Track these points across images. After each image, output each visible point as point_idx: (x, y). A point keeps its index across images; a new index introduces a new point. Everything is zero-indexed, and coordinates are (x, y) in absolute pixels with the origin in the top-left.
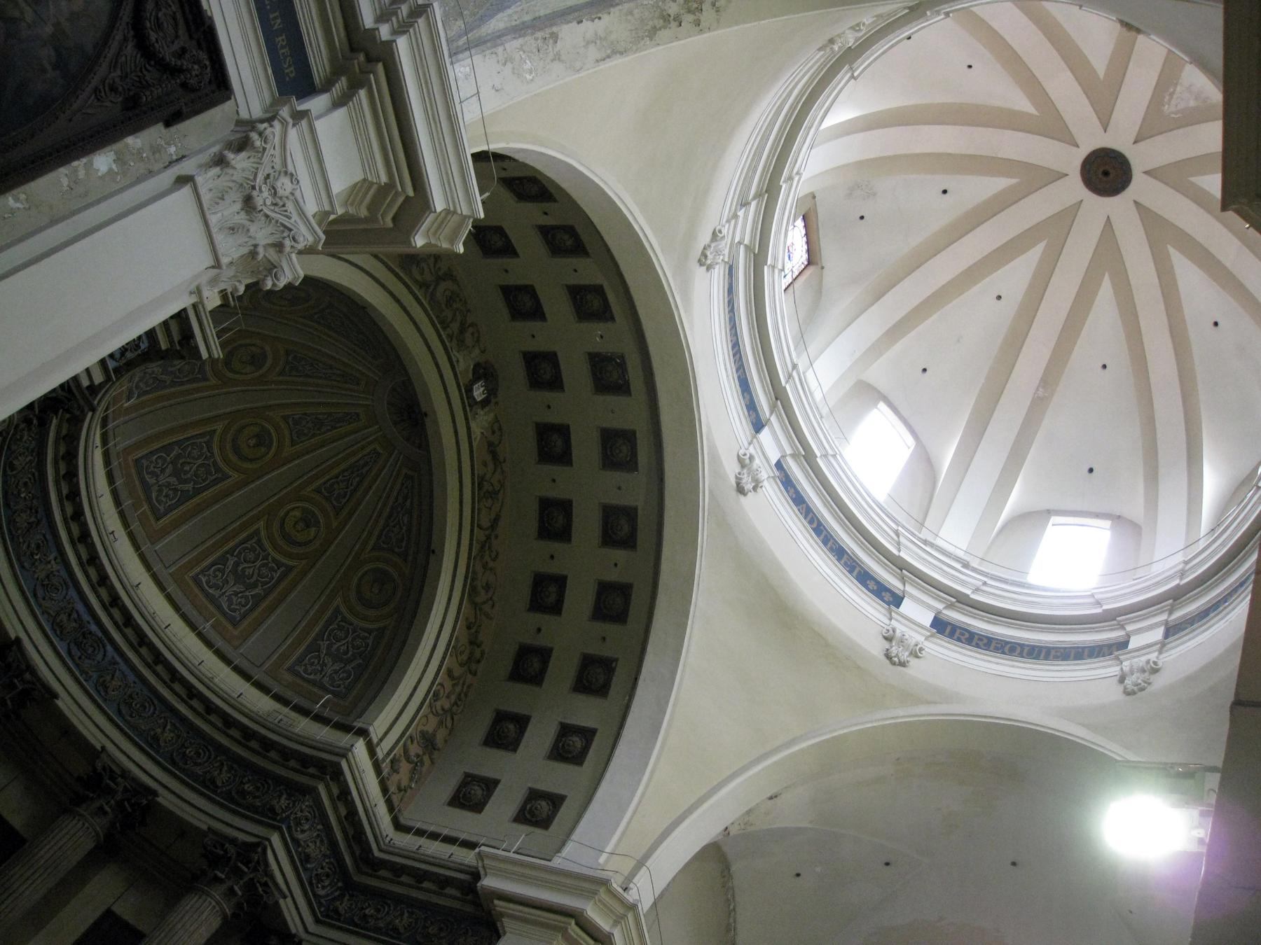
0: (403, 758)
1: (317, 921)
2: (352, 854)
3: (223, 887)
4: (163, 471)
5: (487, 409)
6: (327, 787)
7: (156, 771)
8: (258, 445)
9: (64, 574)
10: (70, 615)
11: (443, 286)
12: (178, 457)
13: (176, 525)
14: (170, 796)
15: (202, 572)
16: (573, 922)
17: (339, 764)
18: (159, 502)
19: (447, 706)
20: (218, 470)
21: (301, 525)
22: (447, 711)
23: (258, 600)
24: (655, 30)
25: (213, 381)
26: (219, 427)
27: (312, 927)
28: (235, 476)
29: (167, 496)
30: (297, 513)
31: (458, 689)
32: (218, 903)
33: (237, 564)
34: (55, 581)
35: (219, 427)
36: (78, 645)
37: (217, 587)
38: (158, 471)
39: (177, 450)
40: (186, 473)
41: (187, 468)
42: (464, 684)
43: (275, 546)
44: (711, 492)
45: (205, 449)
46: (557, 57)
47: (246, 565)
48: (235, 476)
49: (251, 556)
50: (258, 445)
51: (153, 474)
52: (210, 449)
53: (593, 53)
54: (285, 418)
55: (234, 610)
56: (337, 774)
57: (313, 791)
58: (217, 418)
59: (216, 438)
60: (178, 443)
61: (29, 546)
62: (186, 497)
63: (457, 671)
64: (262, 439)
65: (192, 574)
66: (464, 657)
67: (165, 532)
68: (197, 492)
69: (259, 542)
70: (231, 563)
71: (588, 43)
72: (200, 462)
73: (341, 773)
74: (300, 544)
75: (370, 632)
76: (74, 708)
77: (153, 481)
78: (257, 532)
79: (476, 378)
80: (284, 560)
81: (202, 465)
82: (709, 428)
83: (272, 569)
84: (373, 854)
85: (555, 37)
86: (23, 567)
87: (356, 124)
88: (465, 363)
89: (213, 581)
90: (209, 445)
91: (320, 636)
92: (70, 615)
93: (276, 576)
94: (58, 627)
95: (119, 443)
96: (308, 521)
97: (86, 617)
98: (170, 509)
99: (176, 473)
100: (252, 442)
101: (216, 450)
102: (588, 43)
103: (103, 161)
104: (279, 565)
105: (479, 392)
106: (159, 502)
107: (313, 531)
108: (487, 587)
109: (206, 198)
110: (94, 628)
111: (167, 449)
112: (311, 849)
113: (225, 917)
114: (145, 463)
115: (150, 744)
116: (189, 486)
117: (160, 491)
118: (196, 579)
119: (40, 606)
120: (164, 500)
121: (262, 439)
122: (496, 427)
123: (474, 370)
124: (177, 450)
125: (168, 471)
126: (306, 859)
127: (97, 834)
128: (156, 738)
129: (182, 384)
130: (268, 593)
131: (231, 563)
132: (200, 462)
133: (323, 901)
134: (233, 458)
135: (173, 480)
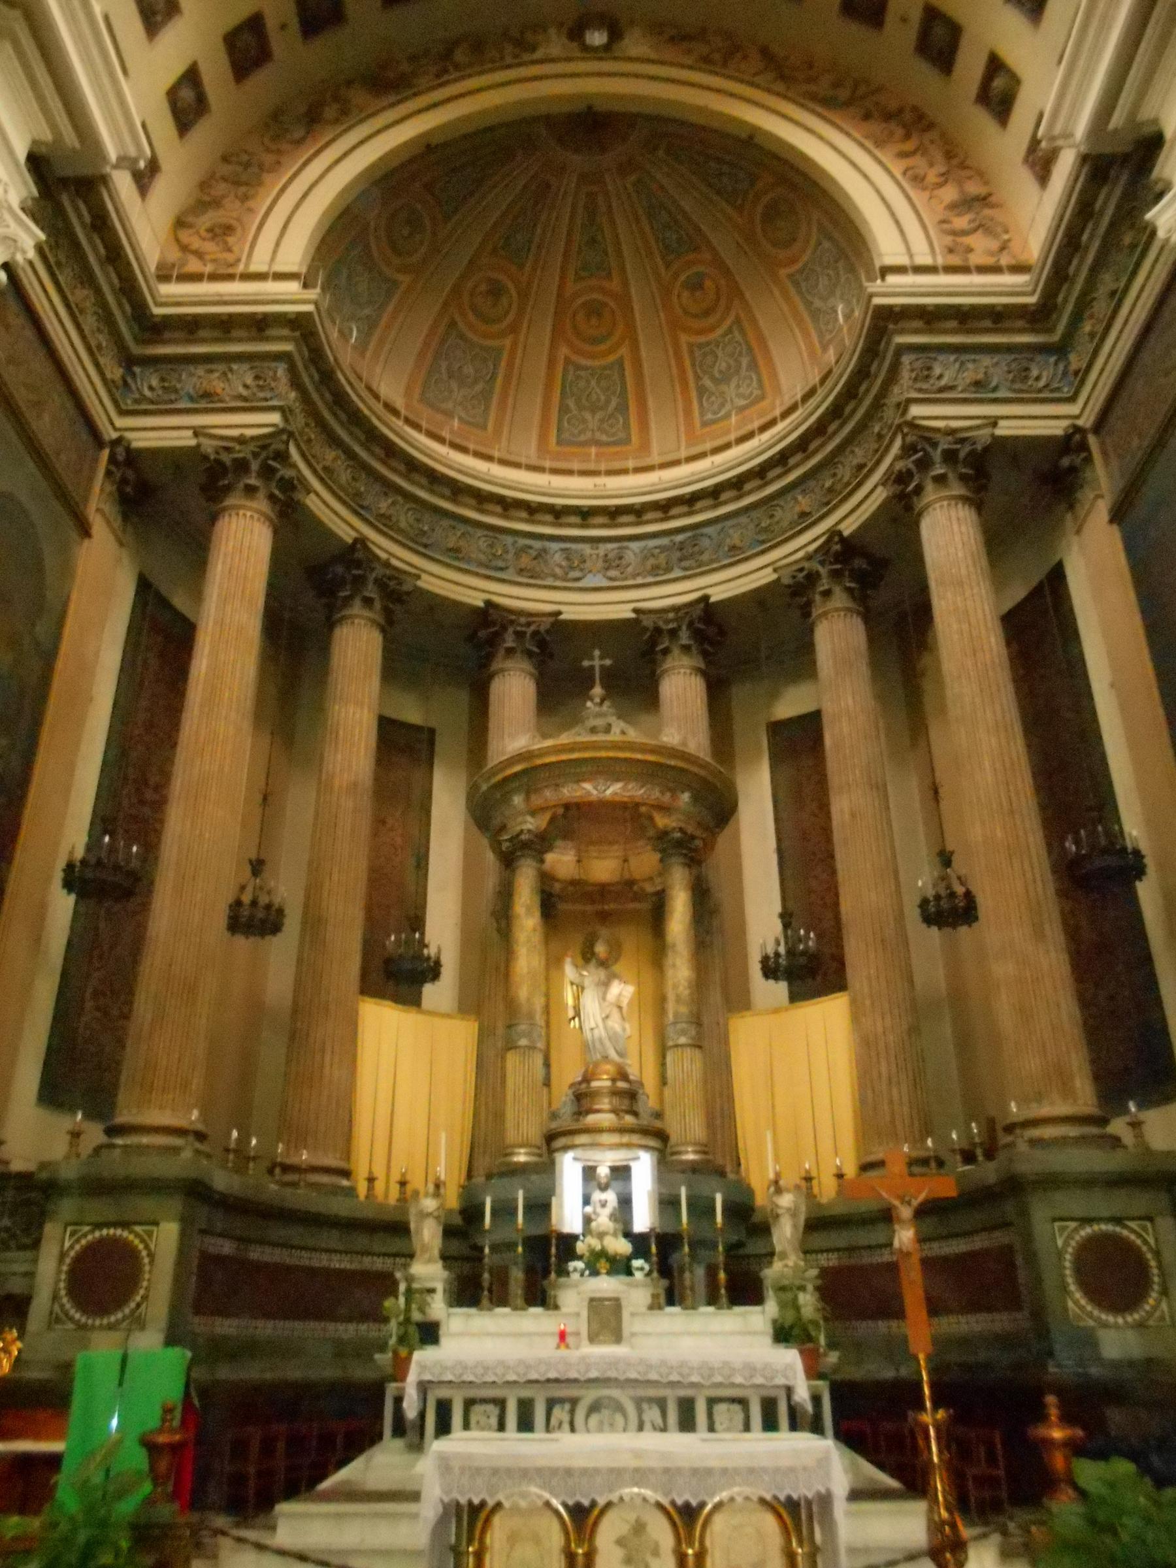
1: (1072, 399)
2: (1021, 331)
3: (929, 487)
8: (599, 315)
9: (610, 546)
10: (653, 555)
12: (578, 402)
15: (702, 414)
18: (614, 435)
19: (943, 169)
20: (610, 367)
21: (698, 294)
22: (948, 172)
27: (1074, 409)
28: (624, 351)
29: (612, 426)
32: (941, 499)
34: (611, 556)
37: (723, 405)
38: (581, 427)
39: (571, 403)
40: (599, 400)
41: (594, 397)
45: (582, 373)
47: (716, 368)
48: (624, 351)
49: (709, 359)
50: (599, 315)
52: (586, 368)
55: (751, 393)
59: (575, 358)
61: (561, 567)
62: (623, 408)
63: (909, 146)
65: (697, 422)
69: (700, 346)
72: (593, 383)
73: (890, 308)
74: (718, 299)
75: (819, 243)
76: (732, 584)
77: (589, 435)
81: (598, 382)
84: (1032, 305)
86: (501, 569)
88: (556, 44)
89: (715, 407)
91: (809, 304)
92: (653, 555)
94: (655, 570)
95: (530, 453)
96: (695, 285)
97: (665, 541)
98: (626, 426)
100: (594, 321)
104: (730, 331)
105: (597, 38)
106: (614, 435)
107: (708, 283)
108: (836, 85)
110: (680, 538)
111: (564, 409)
112: (971, 373)
113: (965, 499)
115: (805, 520)
116: (614, 402)
118: (705, 424)
119: (626, 579)
120: (614, 430)
121: (594, 310)
124: (571, 403)
126: (978, 384)
127: (848, 609)
128: (804, 515)
130: (750, 350)
132: (593, 383)
133: (1056, 385)
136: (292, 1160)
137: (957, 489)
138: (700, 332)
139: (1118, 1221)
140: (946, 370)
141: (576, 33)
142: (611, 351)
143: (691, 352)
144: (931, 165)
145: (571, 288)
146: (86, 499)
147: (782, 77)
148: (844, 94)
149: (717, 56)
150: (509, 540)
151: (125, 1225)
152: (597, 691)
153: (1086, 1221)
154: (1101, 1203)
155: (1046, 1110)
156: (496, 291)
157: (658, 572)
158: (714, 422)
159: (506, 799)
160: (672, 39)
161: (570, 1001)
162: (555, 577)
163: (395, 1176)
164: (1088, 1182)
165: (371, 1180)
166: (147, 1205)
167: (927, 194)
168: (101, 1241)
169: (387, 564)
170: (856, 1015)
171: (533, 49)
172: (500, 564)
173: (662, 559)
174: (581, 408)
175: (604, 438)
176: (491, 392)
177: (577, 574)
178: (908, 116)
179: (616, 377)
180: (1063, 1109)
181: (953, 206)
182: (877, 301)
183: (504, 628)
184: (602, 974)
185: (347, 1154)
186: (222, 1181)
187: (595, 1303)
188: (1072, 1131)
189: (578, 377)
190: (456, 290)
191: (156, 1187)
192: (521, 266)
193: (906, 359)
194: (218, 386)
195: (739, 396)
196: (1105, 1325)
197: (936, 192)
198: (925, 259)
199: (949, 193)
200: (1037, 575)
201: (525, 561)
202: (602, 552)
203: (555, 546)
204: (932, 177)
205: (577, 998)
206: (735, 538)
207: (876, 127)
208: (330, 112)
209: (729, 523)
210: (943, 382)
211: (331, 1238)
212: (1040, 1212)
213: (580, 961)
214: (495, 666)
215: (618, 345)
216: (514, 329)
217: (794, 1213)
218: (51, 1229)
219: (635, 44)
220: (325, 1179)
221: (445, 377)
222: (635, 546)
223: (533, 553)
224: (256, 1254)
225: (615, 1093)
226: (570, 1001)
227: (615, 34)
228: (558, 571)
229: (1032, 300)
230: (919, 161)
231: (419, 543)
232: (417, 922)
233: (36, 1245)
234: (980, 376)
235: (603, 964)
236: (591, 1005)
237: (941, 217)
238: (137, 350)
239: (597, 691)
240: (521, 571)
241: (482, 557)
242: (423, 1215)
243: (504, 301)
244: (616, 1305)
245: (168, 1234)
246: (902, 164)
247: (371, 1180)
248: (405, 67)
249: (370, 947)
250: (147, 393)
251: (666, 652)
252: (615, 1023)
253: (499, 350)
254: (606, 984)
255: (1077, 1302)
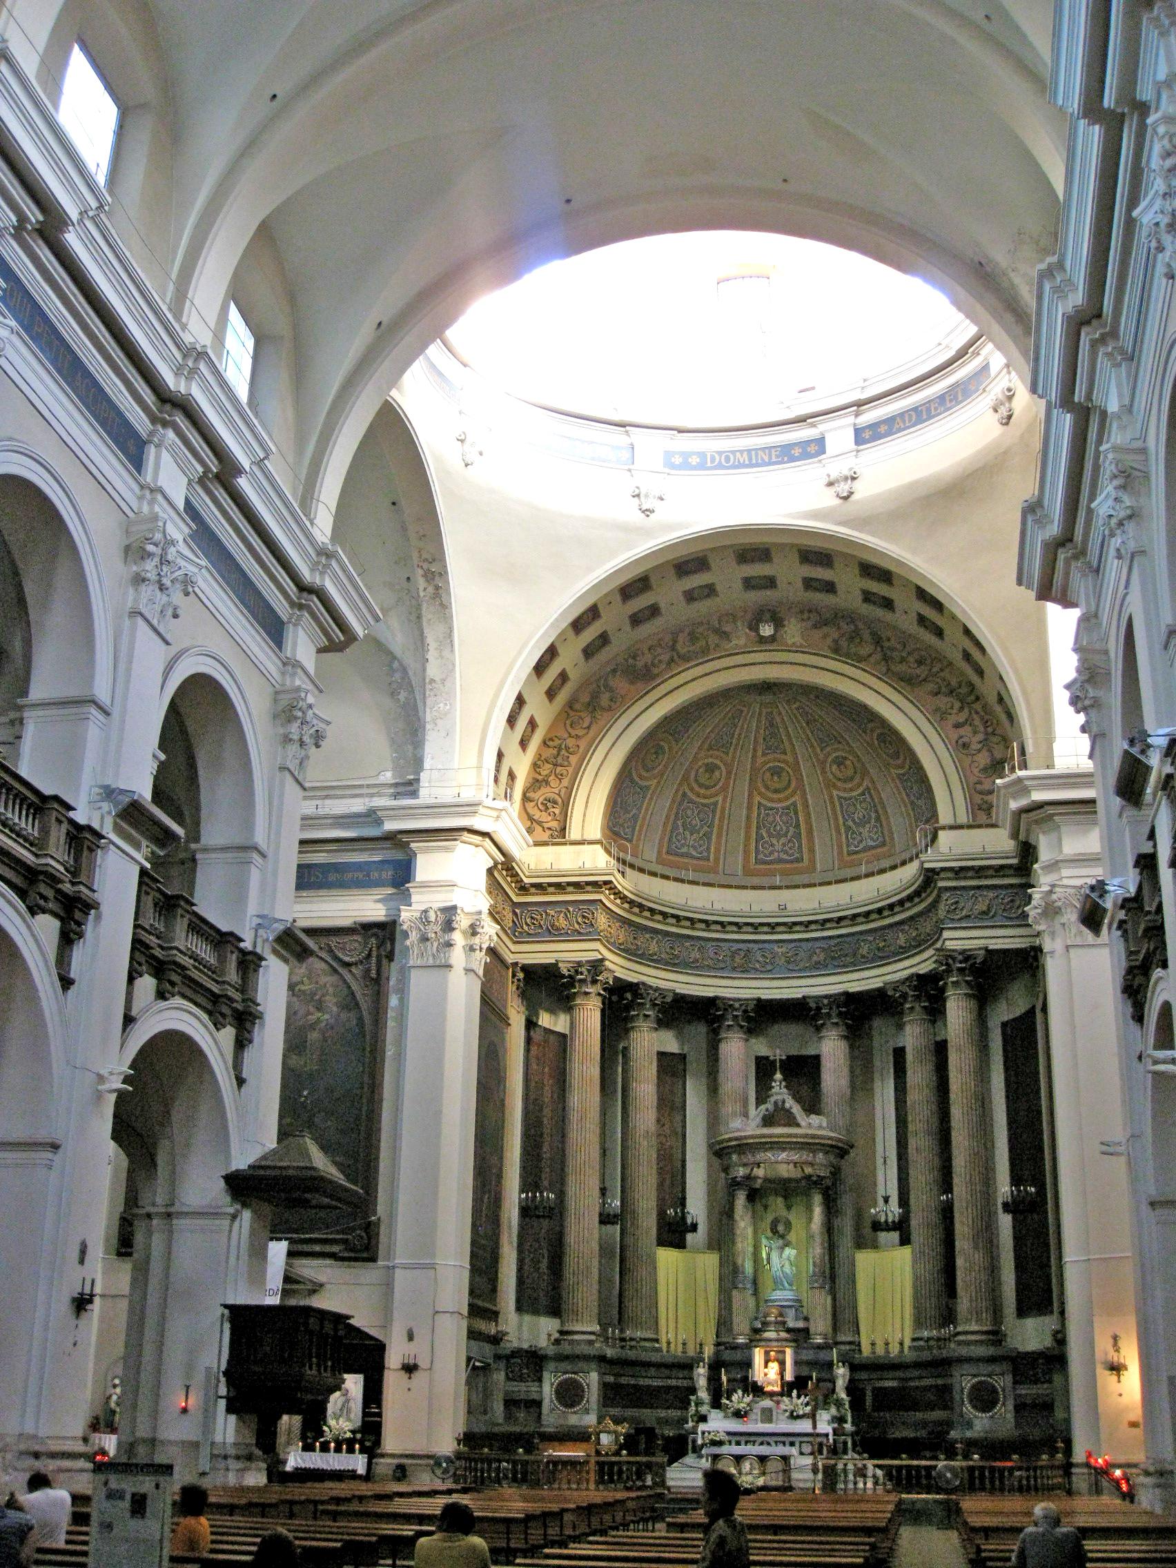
0: (986, 798)
4: (772, 845)
5: (786, 623)
6: (943, 879)
7: (907, 963)
8: (779, 777)
11: (679, 647)
12: (768, 832)
13: (812, 850)
14: (923, 965)
15: (848, 846)
16: (1024, 816)
17: (928, 870)
19: (981, 737)
20: (788, 808)
23: (878, 819)
24: (442, 604)
25: (720, 799)
26: (757, 799)
28: (796, 798)
30: (834, 767)
31: (977, 722)
33: (853, 821)
35: (757, 799)
36: (833, 958)
42: (977, 713)
43: (851, 790)
44: (840, 524)
46: (443, 681)
49: (852, 809)
50: (779, 777)
51: (771, 853)
53: (446, 653)
54: (764, 754)
56: (932, 870)
57: (940, 888)
58: (750, 796)
60: (758, 828)
62: (798, 835)
64: (777, 772)
66: (957, 705)
67: (812, 861)
68: (798, 826)
70: (850, 823)
71: (442, 657)
72: (778, 818)
78: (840, 798)
79: (757, 630)
80: (861, 789)
82: (790, 515)
83: (865, 800)
85: (432, 681)
87: (427, 850)
88: (742, 636)
90: (767, 808)
93: (869, 800)
94: (817, 966)
96: (840, 762)
99: (779, 836)
101: (774, 805)
102: (442, 657)
103: (393, 1001)
104: (863, 794)
105: (767, 630)
107: (848, 762)
108: (920, 662)
109: (419, 963)
110: (833, 942)
111: (759, 838)
114: (761, 856)
117: (786, 853)
118: (849, 854)
121: (777, 772)
122: (806, 616)
123: (750, 629)
125: (774, 841)
129: (713, 821)
131: (850, 823)
132: (778, 818)
134: (781, 796)
135: (783, 840)
136: (633, 1336)
137: (965, 990)
138: (845, 790)
139: (989, 1376)
140: (967, 906)
141: (754, 627)
142: (787, 798)
143: (841, 805)
144: (975, 733)
145: (760, 760)
146: (505, 1007)
147: (886, 659)
148: (922, 671)
149: (844, 643)
150: (727, 944)
151: (575, 1373)
152: (778, 1076)
153: (975, 1376)
154: (985, 1368)
155: (967, 1328)
156: (711, 769)
157: (817, 968)
158: (856, 853)
159: (730, 1153)
160: (815, 626)
161: (764, 1255)
162: (756, 970)
163: (680, 1341)
164: (979, 1360)
165: (669, 1343)
166: (581, 1365)
167: (968, 761)
168: (566, 1380)
169: (657, 989)
170: (914, 1261)
171: (725, 636)
172: (722, 965)
173: (822, 956)
174: (770, 835)
175: (785, 857)
176: (711, 832)
177: (769, 968)
178: (964, 690)
179: (792, 814)
180: (976, 1328)
181: (985, 770)
182: (927, 865)
183: (726, 1010)
184: (781, 1242)
185: (657, 1331)
186: (609, 1352)
187: (764, 1410)
188: (983, 1337)
189: (768, 815)
190: (685, 778)
191: (587, 1358)
192: (727, 754)
193: (945, 896)
194: (562, 922)
195: (872, 839)
196: (976, 1417)
197: (975, 758)
198: (963, 818)
199: (983, 759)
200: (1028, 1007)
201: (737, 959)
202: (784, 950)
203: (756, 946)
204: (975, 746)
205: (768, 1255)
206: (864, 950)
207: (943, 701)
208: (604, 700)
209: (862, 937)
210: (964, 913)
211: (652, 1371)
212: (956, 1374)
213: (770, 1234)
214: (723, 1035)
215: (794, 793)
216: (724, 789)
217: (844, 1376)
218: (546, 1375)
219: (793, 631)
220: (647, 1344)
221: (681, 830)
222: (804, 944)
223: (742, 954)
224: (624, 1380)
225: (776, 1323)
226: (764, 1255)
227: (778, 623)
228: (758, 966)
229: (1015, 861)
230: (966, 731)
231: (673, 964)
232: (683, 1202)
233: (540, 1380)
234: (985, 908)
235: (782, 1237)
236: (775, 1256)
237: (976, 780)
238: (516, 899)
239: (778, 1076)
240: (734, 969)
241: (710, 962)
242: (699, 1375)
243: (717, 773)
244: (770, 1410)
245: (594, 1377)
246: (954, 735)
247: (669, 1343)
248: (648, 658)
249: (661, 1214)
250: (526, 928)
251: (823, 1025)
252: (787, 1269)
253: (716, 804)
254: (782, 1249)
255: (968, 1408)
